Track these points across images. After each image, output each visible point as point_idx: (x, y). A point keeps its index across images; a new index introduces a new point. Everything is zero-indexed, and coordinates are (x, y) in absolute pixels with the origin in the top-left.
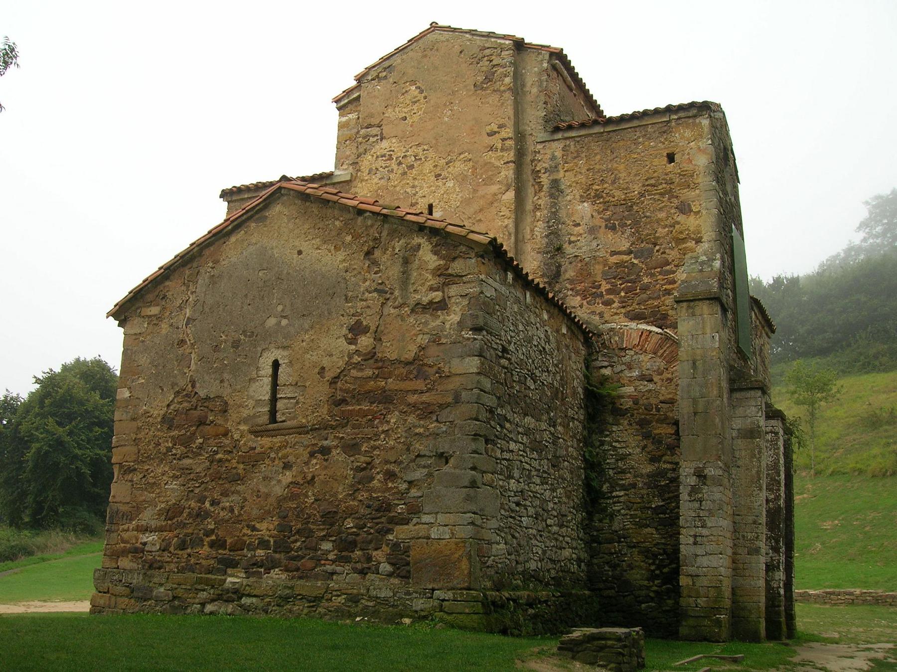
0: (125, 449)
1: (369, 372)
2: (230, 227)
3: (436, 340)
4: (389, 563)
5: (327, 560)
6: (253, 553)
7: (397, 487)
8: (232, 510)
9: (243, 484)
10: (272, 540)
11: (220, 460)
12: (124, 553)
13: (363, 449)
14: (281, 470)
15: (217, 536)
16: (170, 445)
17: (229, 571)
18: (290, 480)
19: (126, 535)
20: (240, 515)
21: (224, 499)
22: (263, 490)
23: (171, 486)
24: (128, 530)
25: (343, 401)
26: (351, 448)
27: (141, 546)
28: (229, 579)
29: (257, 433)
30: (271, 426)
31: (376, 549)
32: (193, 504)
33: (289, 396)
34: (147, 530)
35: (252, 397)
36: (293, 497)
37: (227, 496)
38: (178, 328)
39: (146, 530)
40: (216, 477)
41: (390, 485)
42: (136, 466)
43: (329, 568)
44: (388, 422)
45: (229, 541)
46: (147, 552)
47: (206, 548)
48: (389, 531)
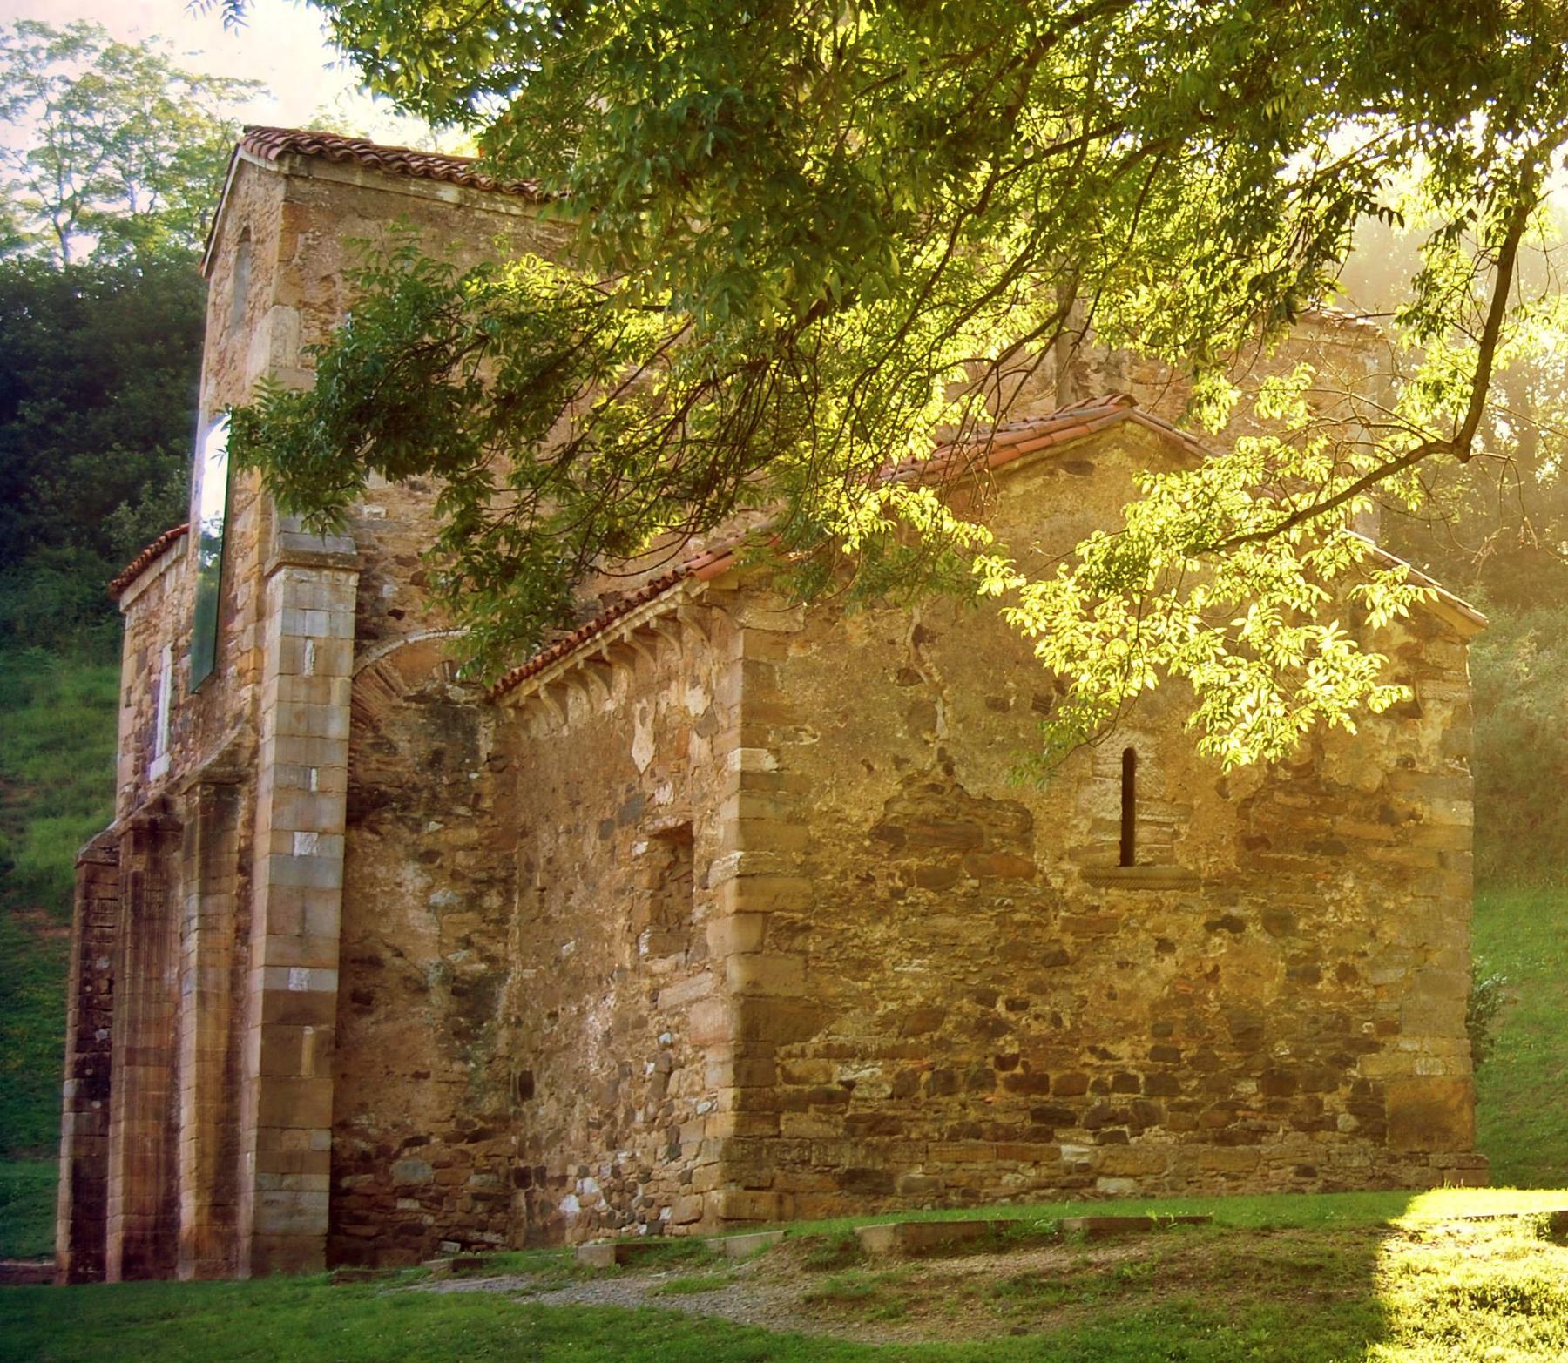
0: (777, 884)
1: (1303, 800)
2: (1017, 465)
3: (1407, 763)
4: (1352, 1113)
5: (1248, 1109)
6: (1105, 1098)
7: (1359, 994)
8: (1056, 1020)
9: (1077, 972)
10: (1142, 1079)
11: (1024, 924)
12: (798, 1103)
13: (1301, 926)
14: (1153, 952)
15: (1025, 1065)
16: (900, 884)
17: (1061, 1133)
18: (1173, 970)
19: (798, 1067)
20: (1075, 1028)
21: (1035, 999)
22: (1121, 985)
23: (910, 969)
24: (803, 1054)
25: (1263, 841)
26: (1279, 923)
27: (840, 1088)
28: (1065, 1148)
29: (1094, 878)
30: (1125, 871)
31: (1329, 1092)
32: (966, 1004)
33: (1160, 818)
34: (853, 1056)
35: (1085, 812)
36: (1185, 1000)
37: (1043, 992)
38: (892, 642)
39: (844, 1054)
40: (1015, 952)
41: (1348, 988)
42: (812, 922)
43: (1254, 1123)
44: (1339, 888)
45: (1053, 1076)
46: (858, 1100)
47: (1001, 1090)
48: (1350, 1063)
